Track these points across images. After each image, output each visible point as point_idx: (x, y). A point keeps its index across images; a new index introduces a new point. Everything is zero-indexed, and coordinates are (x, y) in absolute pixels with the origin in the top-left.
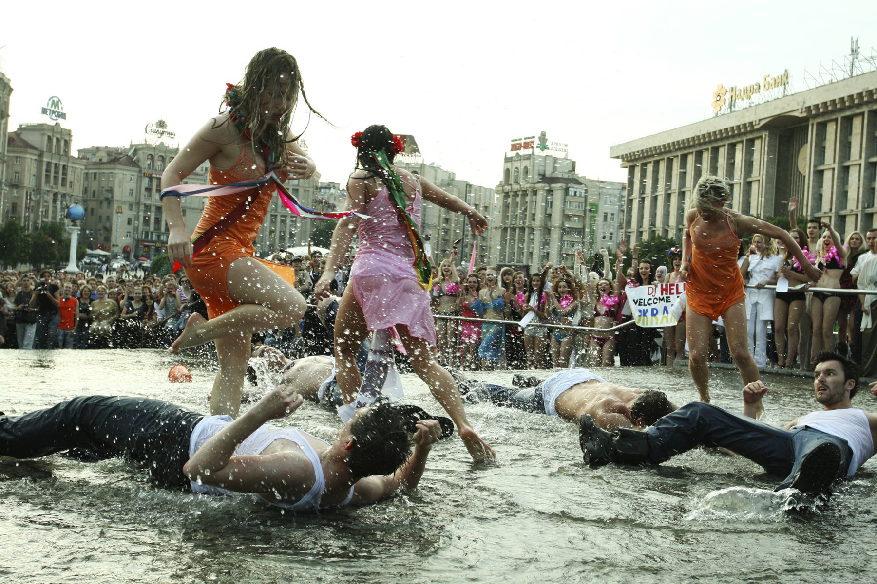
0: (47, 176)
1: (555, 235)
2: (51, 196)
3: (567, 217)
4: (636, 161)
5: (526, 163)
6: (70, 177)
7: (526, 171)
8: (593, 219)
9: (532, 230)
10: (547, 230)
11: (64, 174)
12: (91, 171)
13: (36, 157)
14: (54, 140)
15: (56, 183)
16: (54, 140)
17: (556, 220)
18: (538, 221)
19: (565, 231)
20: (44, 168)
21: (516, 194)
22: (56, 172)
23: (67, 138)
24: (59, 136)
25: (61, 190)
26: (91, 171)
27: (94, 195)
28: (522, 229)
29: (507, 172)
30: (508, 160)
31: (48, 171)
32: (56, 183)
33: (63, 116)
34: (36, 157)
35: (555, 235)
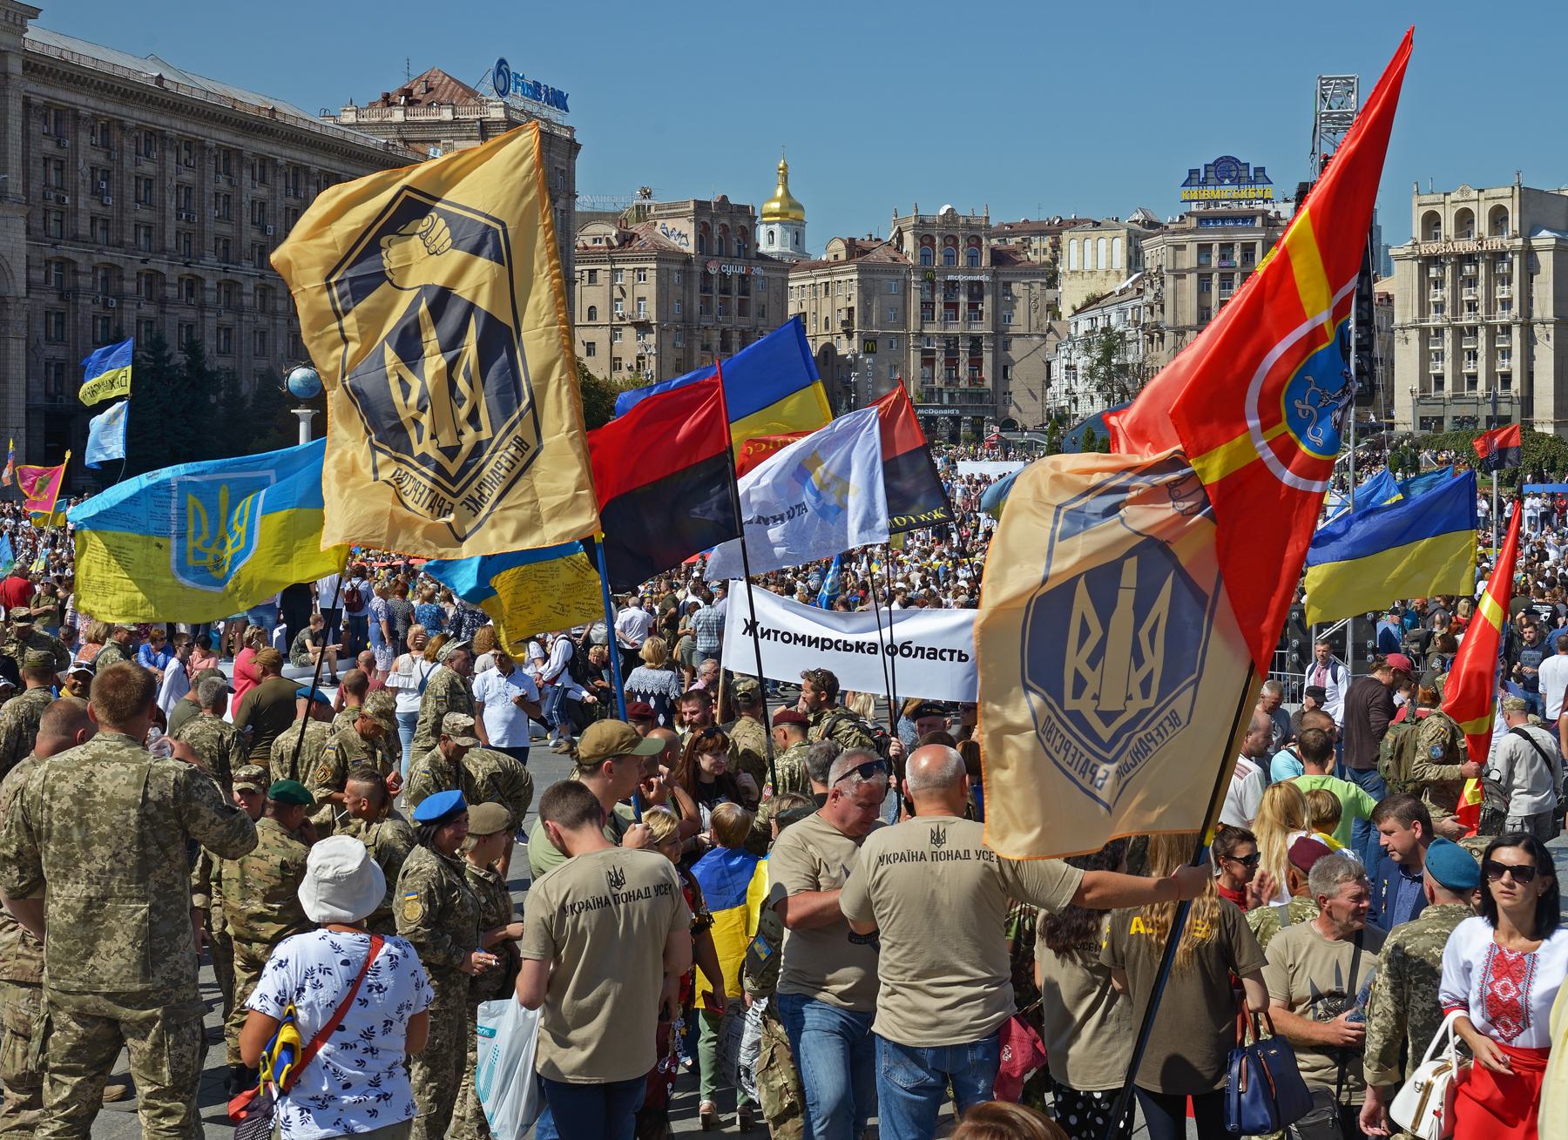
0: (706, 302)
2: (716, 339)
6: (757, 296)
11: (744, 291)
12: (819, 281)
13: (677, 267)
14: (716, 230)
15: (725, 312)
16: (716, 230)
20: (697, 285)
22: (725, 291)
23: (744, 223)
24: (725, 221)
25: (736, 322)
26: (819, 281)
27: (827, 327)
31: (705, 289)
32: (725, 312)
34: (677, 267)
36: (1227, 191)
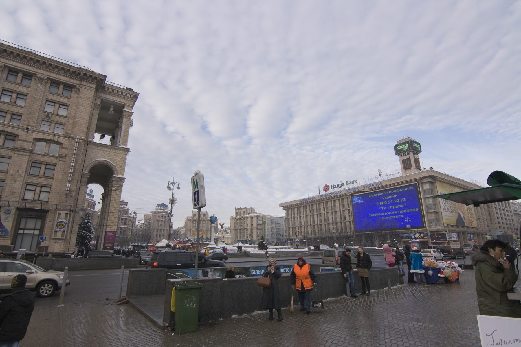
1: (255, 231)
3: (258, 225)
4: (288, 207)
5: (244, 210)
7: (244, 212)
8: (265, 225)
9: (247, 230)
10: (252, 229)
17: (255, 225)
18: (249, 227)
19: (258, 229)
21: (240, 219)
28: (244, 229)
29: (237, 213)
30: (236, 210)
33: (93, 196)
35: (255, 231)
36: (162, 208)
